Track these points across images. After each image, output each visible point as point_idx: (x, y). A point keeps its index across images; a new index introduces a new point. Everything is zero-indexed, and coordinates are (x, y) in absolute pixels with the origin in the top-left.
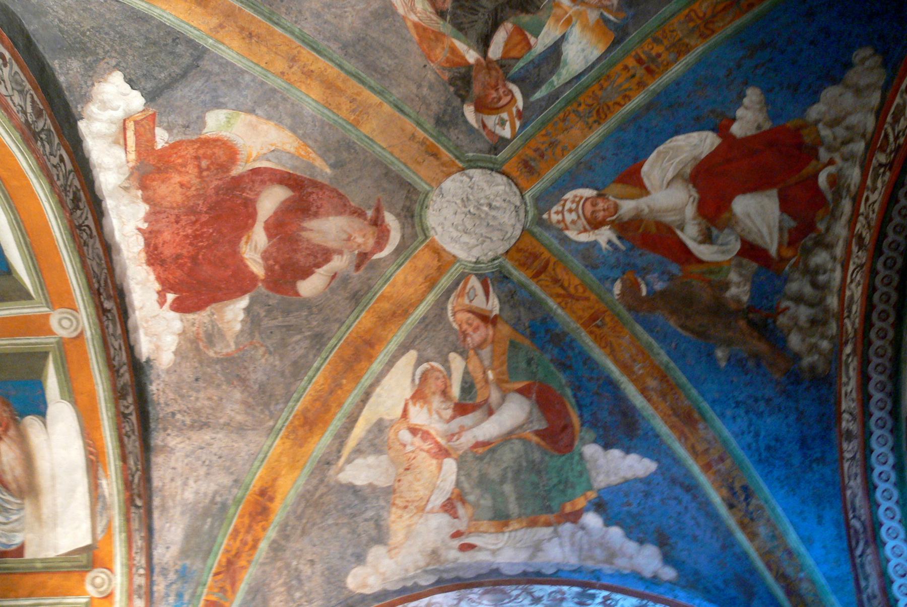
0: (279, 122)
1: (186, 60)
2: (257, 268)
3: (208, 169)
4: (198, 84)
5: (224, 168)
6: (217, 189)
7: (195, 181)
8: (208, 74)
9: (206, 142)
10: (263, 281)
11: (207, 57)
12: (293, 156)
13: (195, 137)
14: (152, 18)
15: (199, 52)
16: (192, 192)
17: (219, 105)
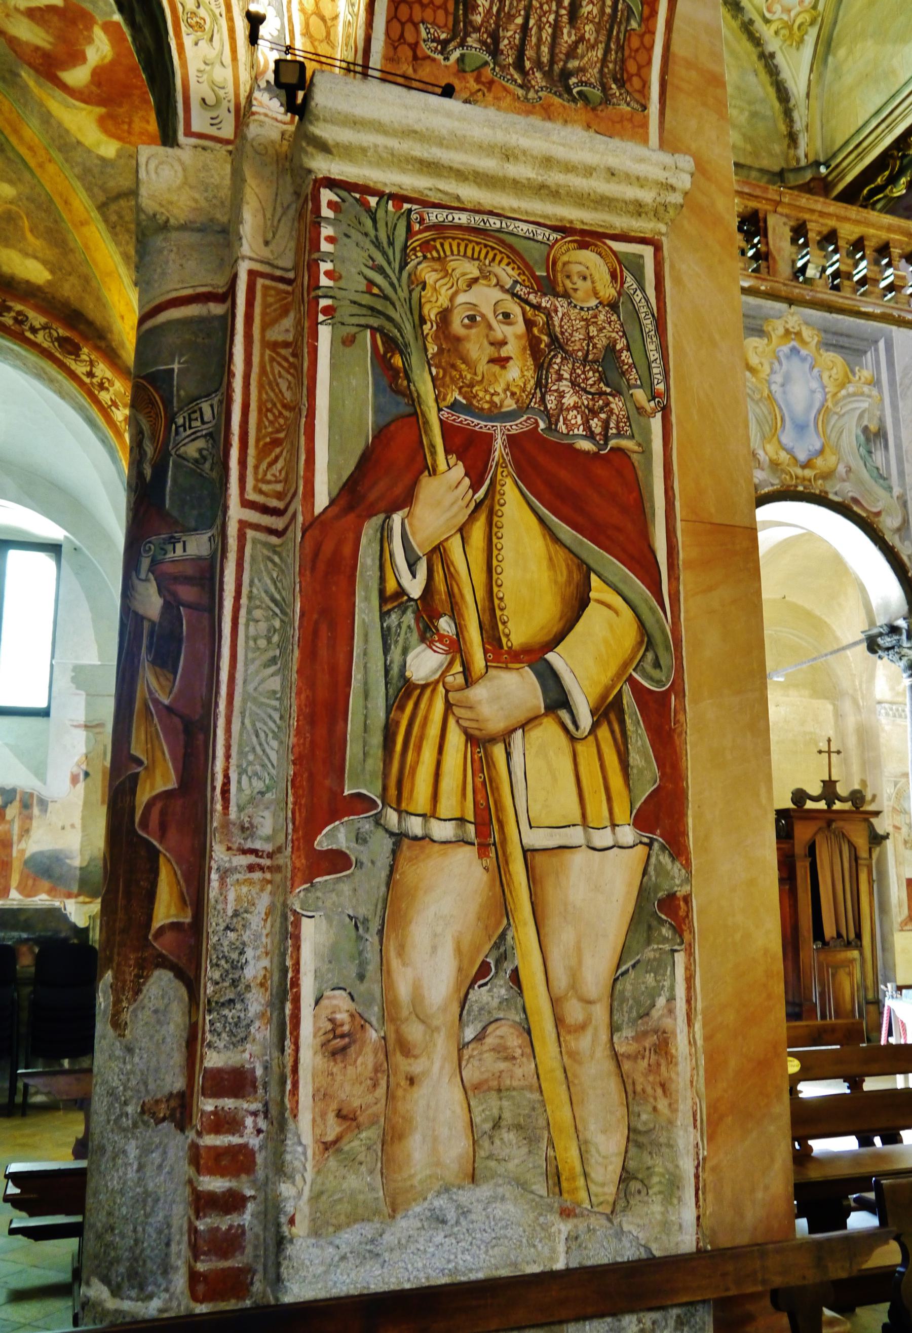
0: (60, 125)
1: (113, 207)
2: (98, 33)
3: (123, 122)
4: (111, 184)
5: (111, 116)
6: (120, 105)
7: (136, 119)
8: (103, 188)
9: (119, 138)
10: (96, 23)
11: (99, 203)
12: (53, 97)
13: (127, 146)
14: (121, 253)
15: (102, 207)
16: (141, 113)
17: (103, 159)
